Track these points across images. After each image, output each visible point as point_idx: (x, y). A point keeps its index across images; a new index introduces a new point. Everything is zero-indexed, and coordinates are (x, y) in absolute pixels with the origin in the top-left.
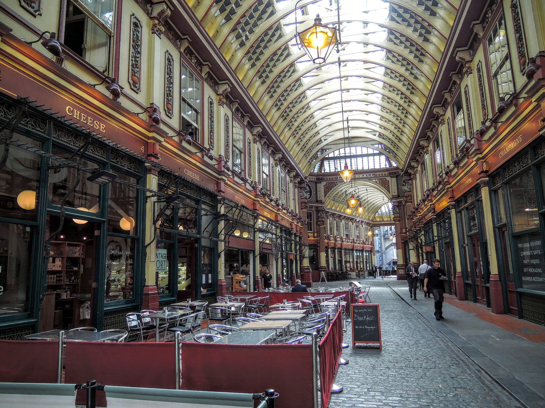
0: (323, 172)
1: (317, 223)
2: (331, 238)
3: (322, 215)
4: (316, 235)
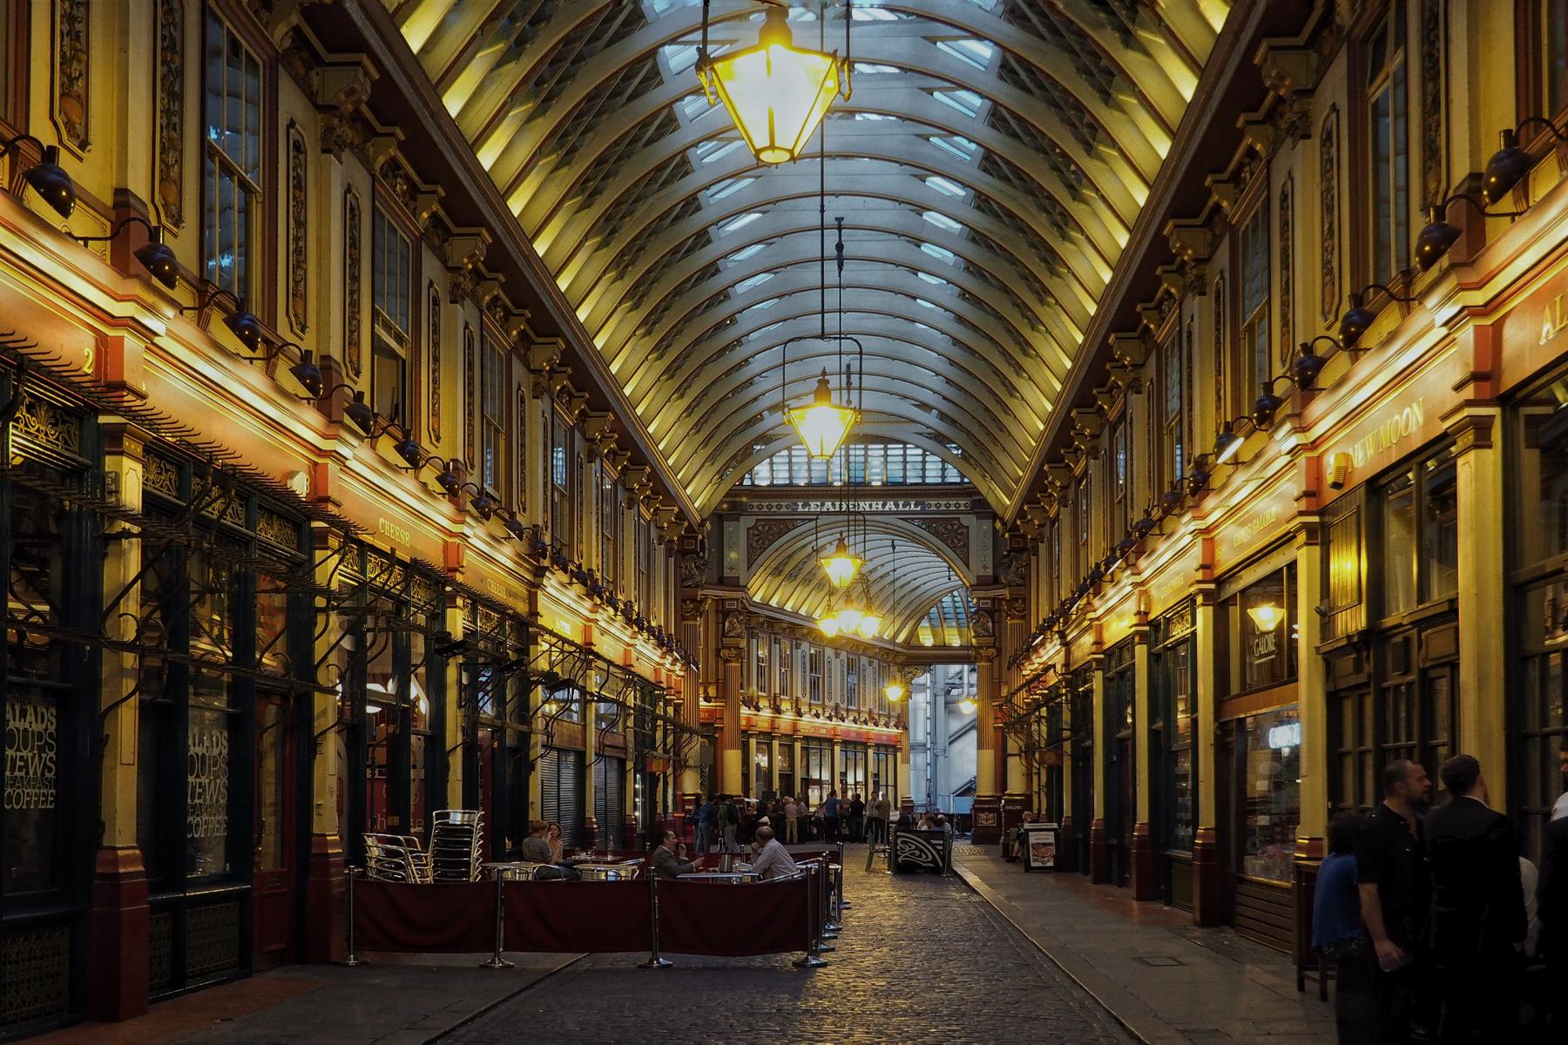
0: (747, 482)
1: (718, 651)
2: (763, 703)
3: (735, 628)
4: (712, 691)
